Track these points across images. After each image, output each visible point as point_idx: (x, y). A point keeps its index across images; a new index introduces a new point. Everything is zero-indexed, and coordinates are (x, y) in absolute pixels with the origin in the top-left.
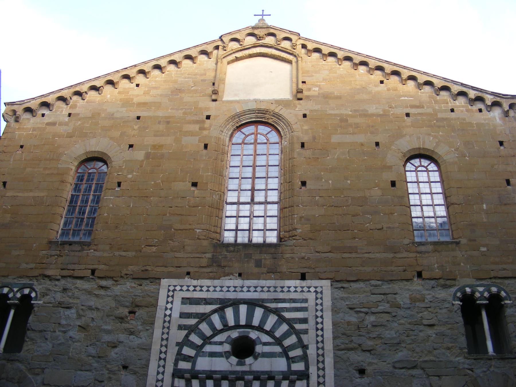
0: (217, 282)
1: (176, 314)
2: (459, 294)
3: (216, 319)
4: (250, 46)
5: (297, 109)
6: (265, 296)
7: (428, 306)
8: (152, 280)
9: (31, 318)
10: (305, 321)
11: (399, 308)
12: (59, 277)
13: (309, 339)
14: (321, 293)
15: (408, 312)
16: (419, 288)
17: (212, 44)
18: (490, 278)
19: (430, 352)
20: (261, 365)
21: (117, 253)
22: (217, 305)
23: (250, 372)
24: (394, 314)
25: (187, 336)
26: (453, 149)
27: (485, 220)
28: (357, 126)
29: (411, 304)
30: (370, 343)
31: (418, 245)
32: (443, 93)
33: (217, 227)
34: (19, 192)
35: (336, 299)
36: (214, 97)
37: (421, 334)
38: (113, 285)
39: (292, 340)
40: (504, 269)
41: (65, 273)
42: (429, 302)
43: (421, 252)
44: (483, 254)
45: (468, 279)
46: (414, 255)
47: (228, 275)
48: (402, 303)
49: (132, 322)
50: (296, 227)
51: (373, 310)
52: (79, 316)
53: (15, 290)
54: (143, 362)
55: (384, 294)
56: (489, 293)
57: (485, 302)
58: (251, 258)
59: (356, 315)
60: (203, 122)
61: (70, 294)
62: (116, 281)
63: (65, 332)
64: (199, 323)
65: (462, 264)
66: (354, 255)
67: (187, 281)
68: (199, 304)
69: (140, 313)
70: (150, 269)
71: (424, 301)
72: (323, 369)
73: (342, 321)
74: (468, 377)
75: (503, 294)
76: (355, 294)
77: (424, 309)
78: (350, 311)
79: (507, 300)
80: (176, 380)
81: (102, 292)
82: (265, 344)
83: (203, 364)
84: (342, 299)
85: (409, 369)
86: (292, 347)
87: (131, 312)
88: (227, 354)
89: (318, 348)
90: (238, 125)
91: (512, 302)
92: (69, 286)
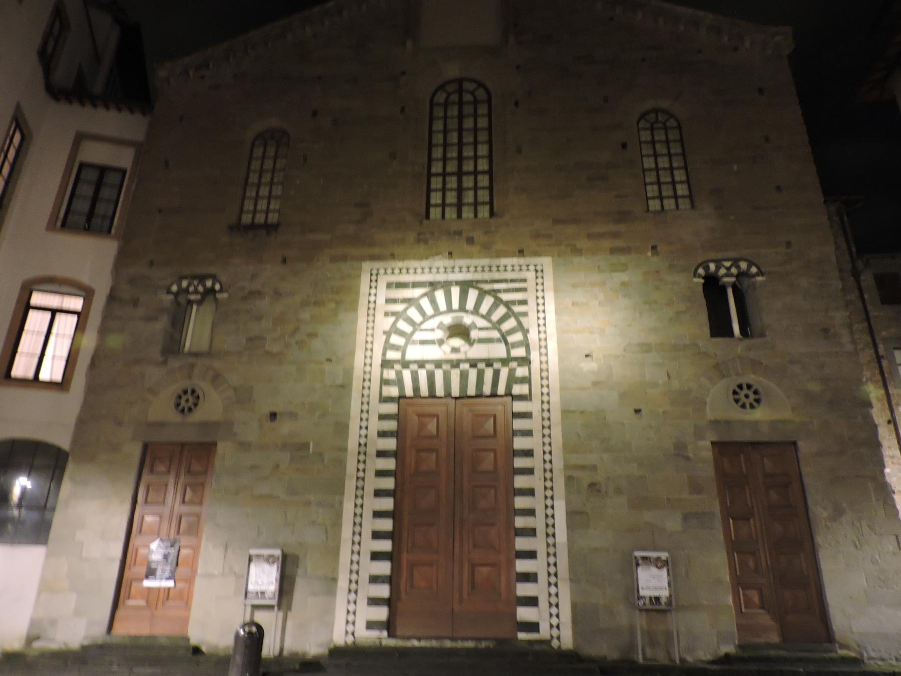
10: (524, 302)
23: (466, 361)
39: (511, 323)
82: (481, 329)
86: (511, 332)
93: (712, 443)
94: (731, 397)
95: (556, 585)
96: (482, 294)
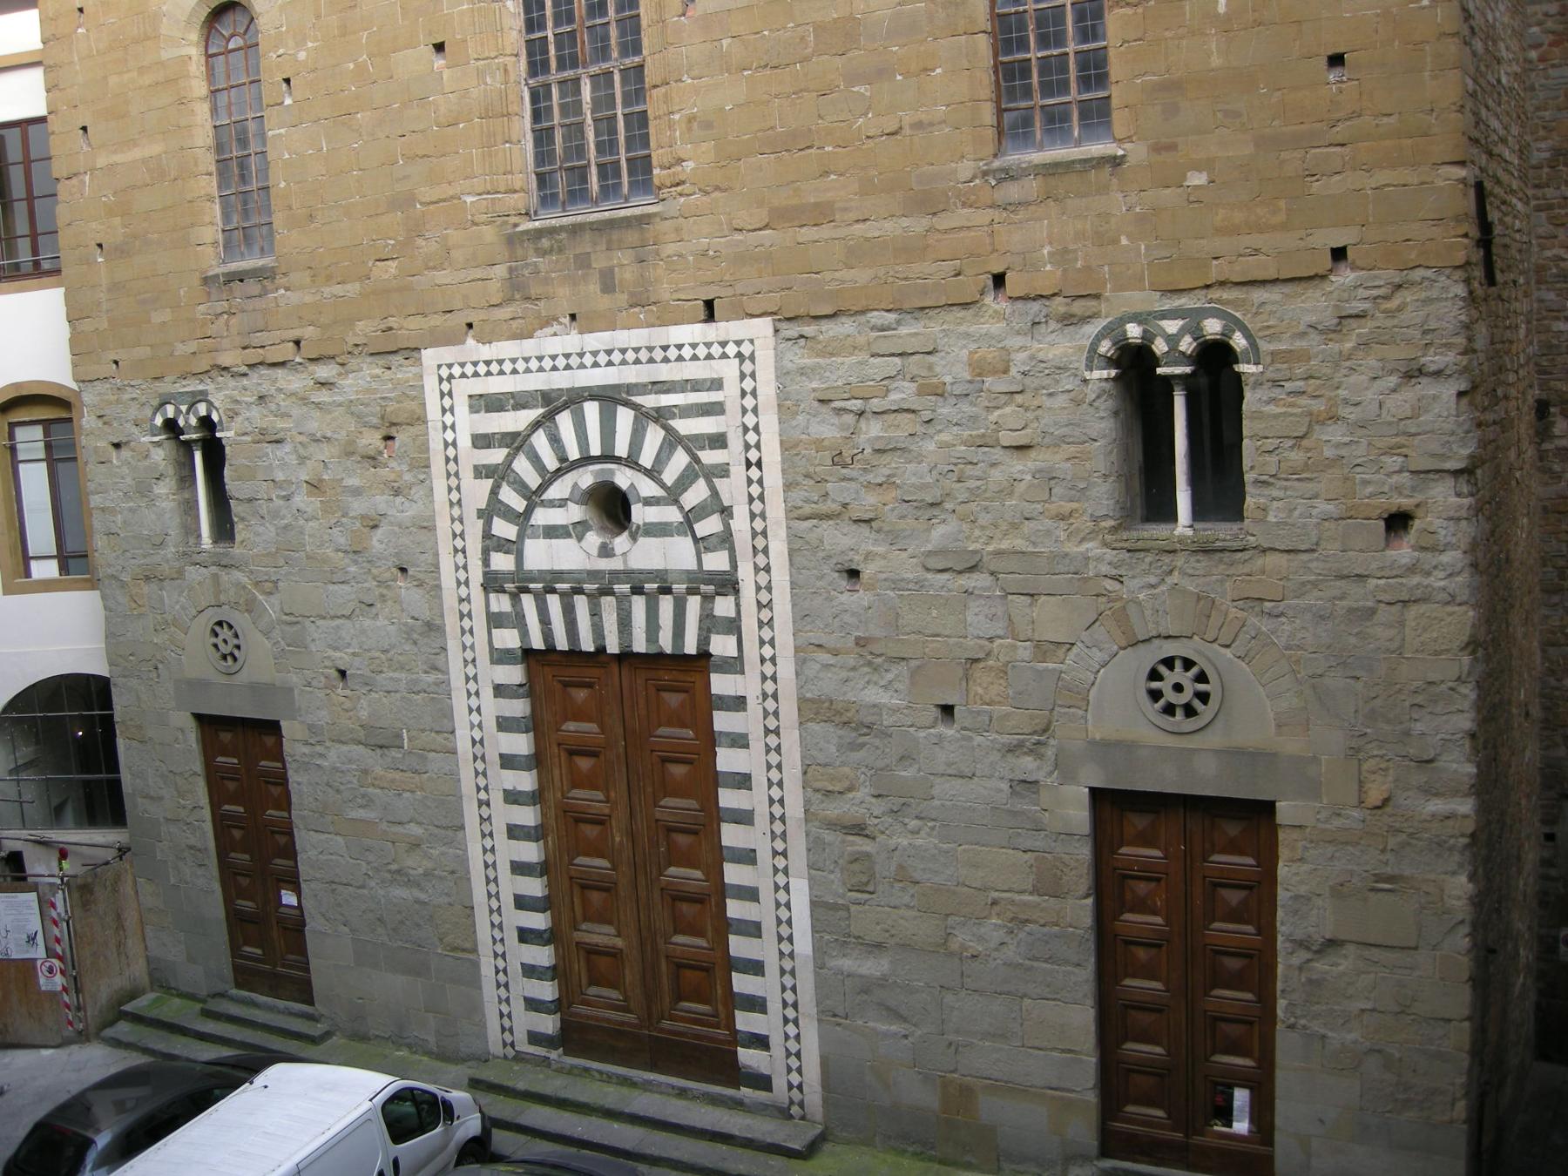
0: (528, 347)
1: (465, 442)
2: (1105, 347)
3: (540, 441)
6: (631, 375)
9: (226, 472)
10: (719, 441)
11: (942, 395)
12: (244, 369)
13: (732, 489)
14: (752, 358)
15: (966, 408)
18: (1208, 287)
19: (1015, 526)
20: (644, 554)
21: (327, 290)
22: (535, 407)
24: (927, 415)
25: (494, 492)
27: (1216, 61)
29: (970, 382)
30: (871, 499)
31: (999, 181)
34: (115, 152)
37: (996, 475)
38: (340, 374)
40: (1257, 251)
41: (253, 356)
42: (1019, 377)
44: (1195, 199)
45: (1137, 294)
46: (983, 216)
47: (547, 322)
48: (948, 379)
49: (393, 464)
51: (876, 404)
52: (302, 460)
53: (184, 408)
54: (429, 558)
55: (900, 355)
57: (1178, 370)
58: (589, 266)
59: (835, 420)
61: (273, 407)
62: (342, 365)
63: (287, 498)
65: (1124, 241)
66: (825, 232)
67: (473, 348)
68: (501, 409)
69: (402, 437)
71: (1006, 371)
72: (767, 569)
73: (804, 437)
74: (1102, 599)
75: (1239, 341)
77: (1004, 398)
78: (824, 409)
80: (492, 596)
81: (324, 396)
82: (649, 502)
83: (540, 555)
84: (802, 371)
85: (960, 572)
88: (579, 528)
89: (753, 516)
92: (266, 388)
93: (1095, 793)
94: (1143, 685)
95: (796, 1022)
96: (645, 417)
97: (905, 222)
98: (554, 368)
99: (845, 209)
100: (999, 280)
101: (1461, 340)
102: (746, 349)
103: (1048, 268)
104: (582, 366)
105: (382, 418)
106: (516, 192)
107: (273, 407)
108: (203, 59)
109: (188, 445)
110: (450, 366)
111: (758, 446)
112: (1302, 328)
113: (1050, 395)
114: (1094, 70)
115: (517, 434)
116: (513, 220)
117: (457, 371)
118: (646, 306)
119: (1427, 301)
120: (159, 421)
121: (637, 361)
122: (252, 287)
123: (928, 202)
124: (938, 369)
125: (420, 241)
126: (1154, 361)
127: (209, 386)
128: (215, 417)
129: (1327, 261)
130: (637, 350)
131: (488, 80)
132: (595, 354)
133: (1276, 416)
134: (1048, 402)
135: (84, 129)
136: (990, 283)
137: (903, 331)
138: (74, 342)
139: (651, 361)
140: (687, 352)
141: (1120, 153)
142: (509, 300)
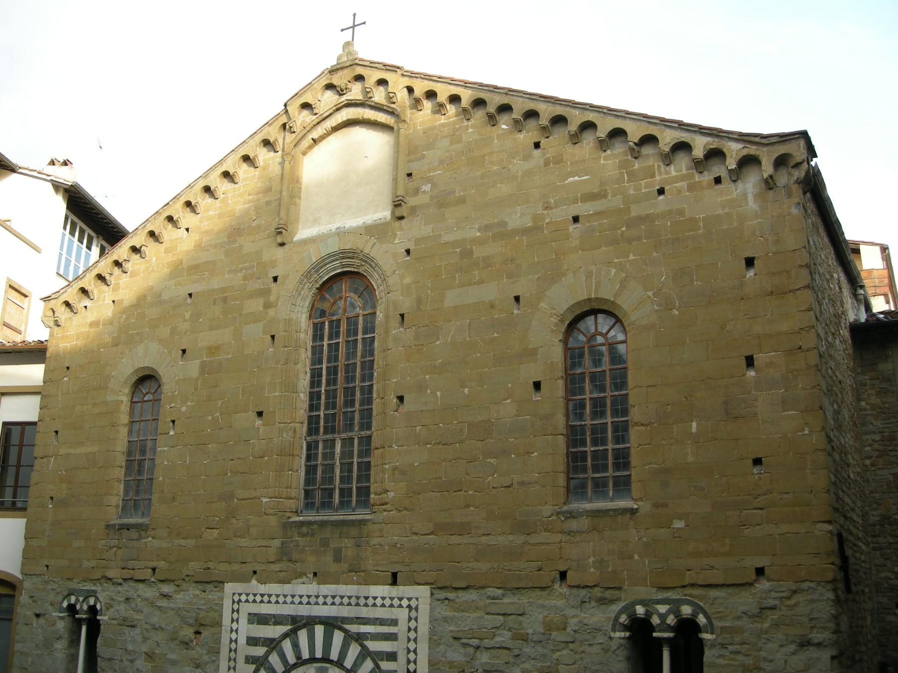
0: (287, 588)
1: (242, 640)
2: (623, 619)
3: (287, 645)
4: (331, 111)
5: (397, 241)
7: (569, 639)
8: (216, 584)
9: (99, 640)
10: (392, 656)
11: (526, 640)
12: (120, 581)
14: (417, 609)
15: (540, 649)
16: (560, 603)
17: (276, 123)
18: (684, 587)
21: (176, 542)
22: (287, 624)
24: (516, 652)
26: (650, 293)
27: (690, 459)
28: (487, 262)
29: (543, 634)
31: (566, 518)
32: (647, 150)
33: (290, 487)
34: (71, 447)
35: (436, 620)
36: (279, 239)
41: (127, 574)
42: (572, 633)
43: (570, 533)
46: (557, 538)
48: (530, 631)
49: (198, 648)
50: (388, 488)
51: (487, 643)
52: (145, 639)
53: (81, 599)
55: (503, 615)
56: (676, 617)
58: (328, 546)
59: (462, 650)
60: (266, 292)
61: (133, 605)
62: (178, 586)
63: (132, 661)
64: (267, 654)
65: (636, 557)
66: (465, 539)
69: (206, 633)
70: (212, 567)
71: (565, 629)
75: (701, 620)
76: (463, 611)
77: (562, 645)
78: (456, 643)
79: (707, 632)
81: (164, 603)
84: (445, 620)
87: (198, 633)
90: (318, 286)
91: (714, 636)
92: (131, 593)
96: (350, 638)
97: (511, 537)
98: (301, 603)
99: (478, 528)
100: (563, 575)
101: (832, 625)
102: (413, 603)
103: (592, 570)
104: (317, 604)
105: (196, 620)
106: (291, 498)
107: (133, 605)
108: (129, 404)
109: (79, 622)
110: (240, 595)
111: (415, 662)
112: (739, 613)
113: (590, 645)
114: (622, 460)
115: (274, 640)
116: (287, 514)
117: (243, 598)
118: (360, 573)
119: (812, 601)
120: (65, 604)
121: (349, 604)
122: (134, 534)
123: (525, 527)
124: (525, 625)
125: (233, 520)
126: (652, 629)
127: (98, 588)
128: (98, 607)
129: (753, 576)
130: (350, 597)
131: (285, 435)
132: (325, 597)
133: (723, 666)
134: (588, 649)
135: (57, 432)
136: (558, 576)
137: (506, 600)
138: (26, 551)
139: (357, 604)
140: (379, 602)
141: (636, 507)
142: (279, 560)
